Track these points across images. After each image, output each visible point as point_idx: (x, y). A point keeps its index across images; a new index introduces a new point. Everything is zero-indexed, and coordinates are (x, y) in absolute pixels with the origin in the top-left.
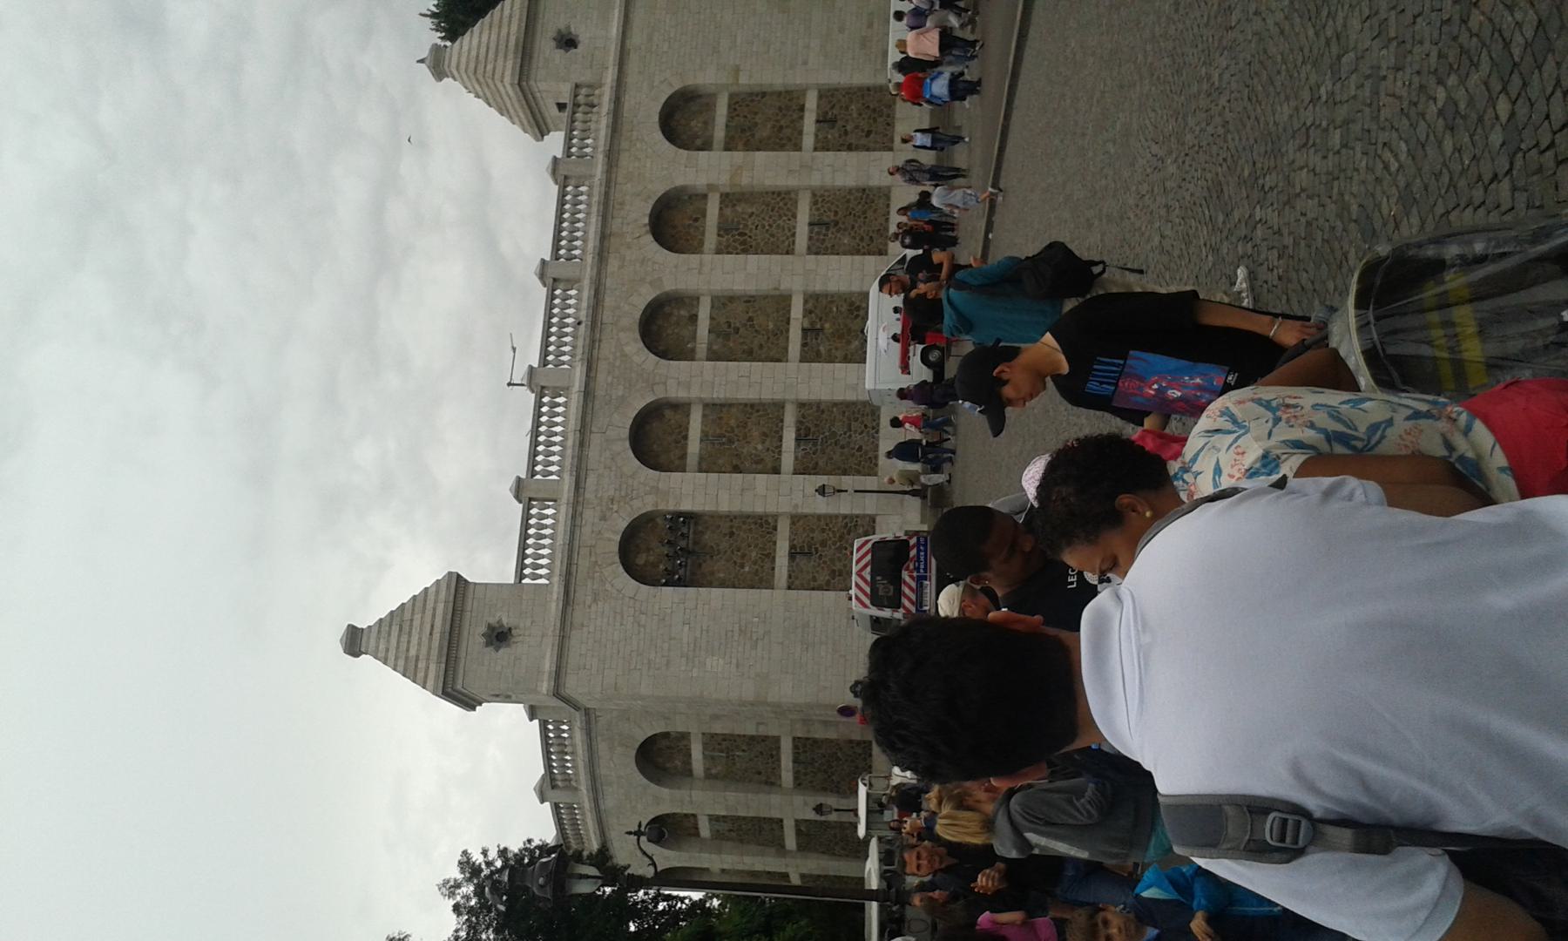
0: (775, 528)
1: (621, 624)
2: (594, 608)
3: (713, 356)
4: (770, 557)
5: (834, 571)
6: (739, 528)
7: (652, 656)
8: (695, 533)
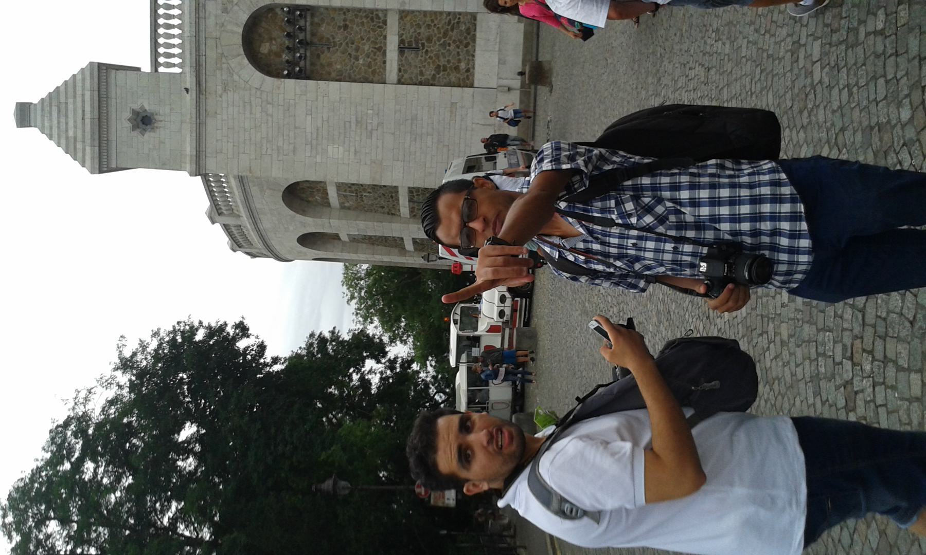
0: (385, 23)
1: (251, 113)
2: (224, 97)
4: (381, 50)
5: (439, 66)
6: (352, 21)
7: (280, 144)
8: (312, 24)
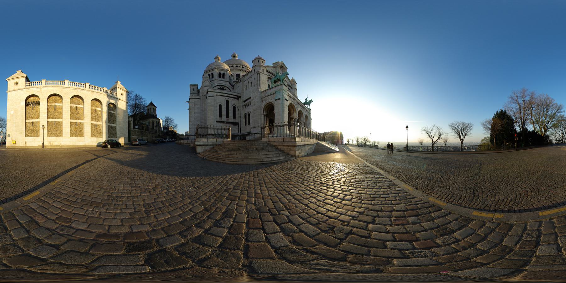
3: (71, 107)
